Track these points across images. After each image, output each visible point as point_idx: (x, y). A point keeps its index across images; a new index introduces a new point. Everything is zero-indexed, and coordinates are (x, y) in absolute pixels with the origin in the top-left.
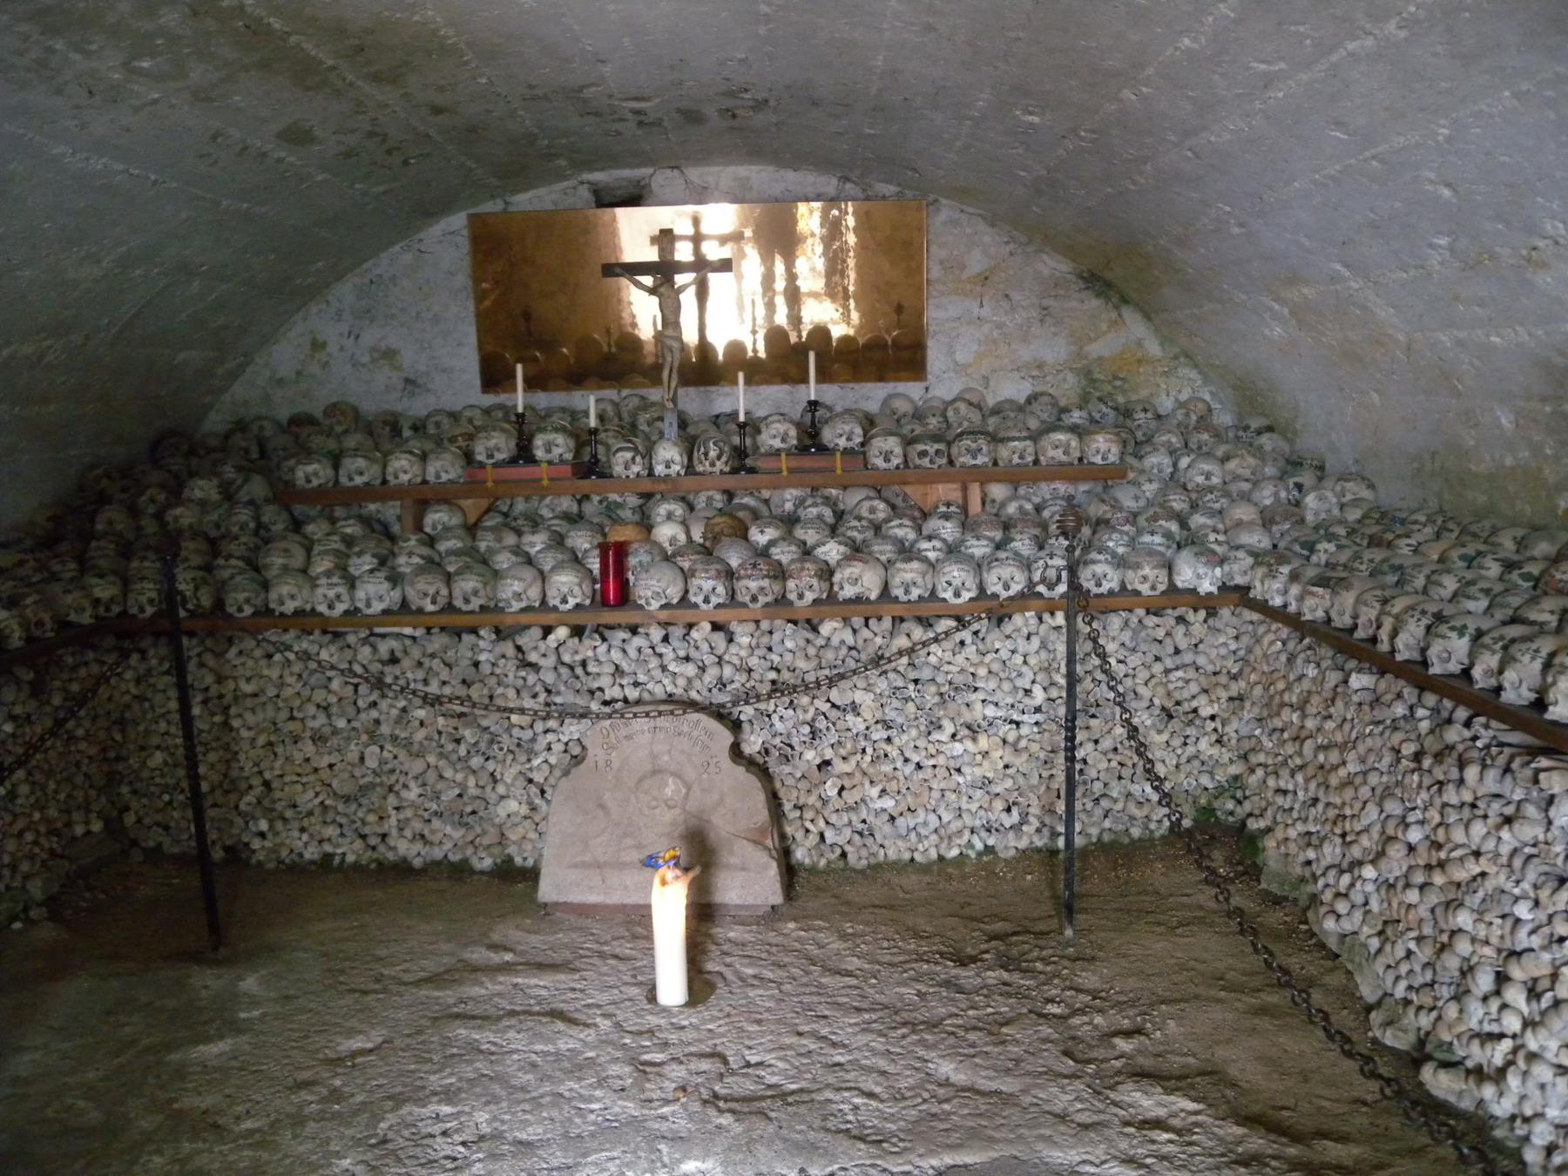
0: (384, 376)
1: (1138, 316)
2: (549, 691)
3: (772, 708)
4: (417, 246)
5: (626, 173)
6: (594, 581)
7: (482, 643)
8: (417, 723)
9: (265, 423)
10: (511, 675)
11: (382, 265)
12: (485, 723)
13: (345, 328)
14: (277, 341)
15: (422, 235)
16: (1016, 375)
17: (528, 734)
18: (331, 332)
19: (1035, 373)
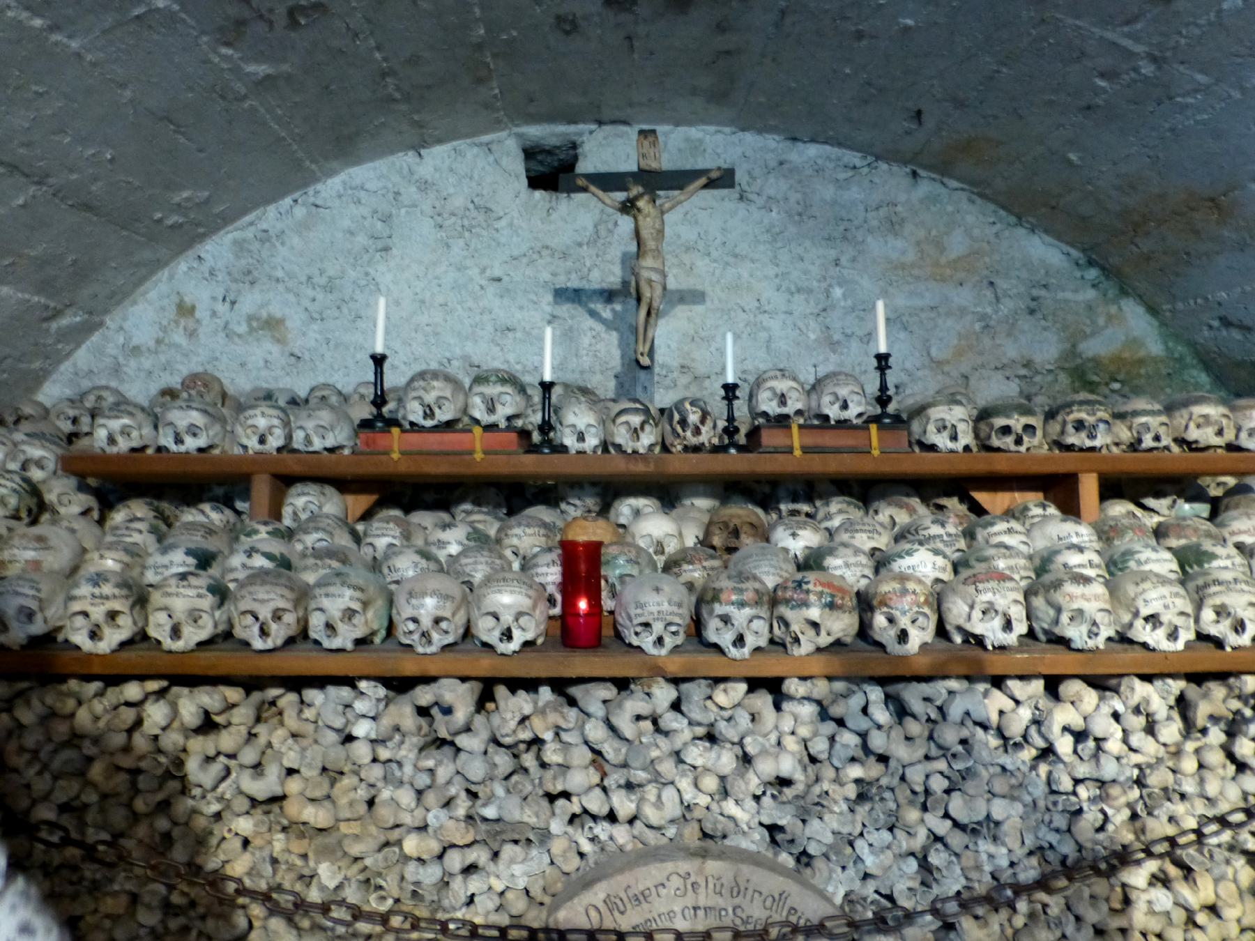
0: (263, 350)
1: (1140, 310)
2: (473, 795)
3: (859, 829)
4: (312, 200)
5: (561, 128)
6: (551, 601)
7: (360, 706)
8: (237, 843)
9: (105, 394)
10: (408, 769)
11: (270, 217)
12: (355, 849)
13: (220, 292)
14: (135, 303)
15: (319, 186)
16: (999, 376)
17: (431, 875)
18: (201, 294)
19: (1023, 372)
